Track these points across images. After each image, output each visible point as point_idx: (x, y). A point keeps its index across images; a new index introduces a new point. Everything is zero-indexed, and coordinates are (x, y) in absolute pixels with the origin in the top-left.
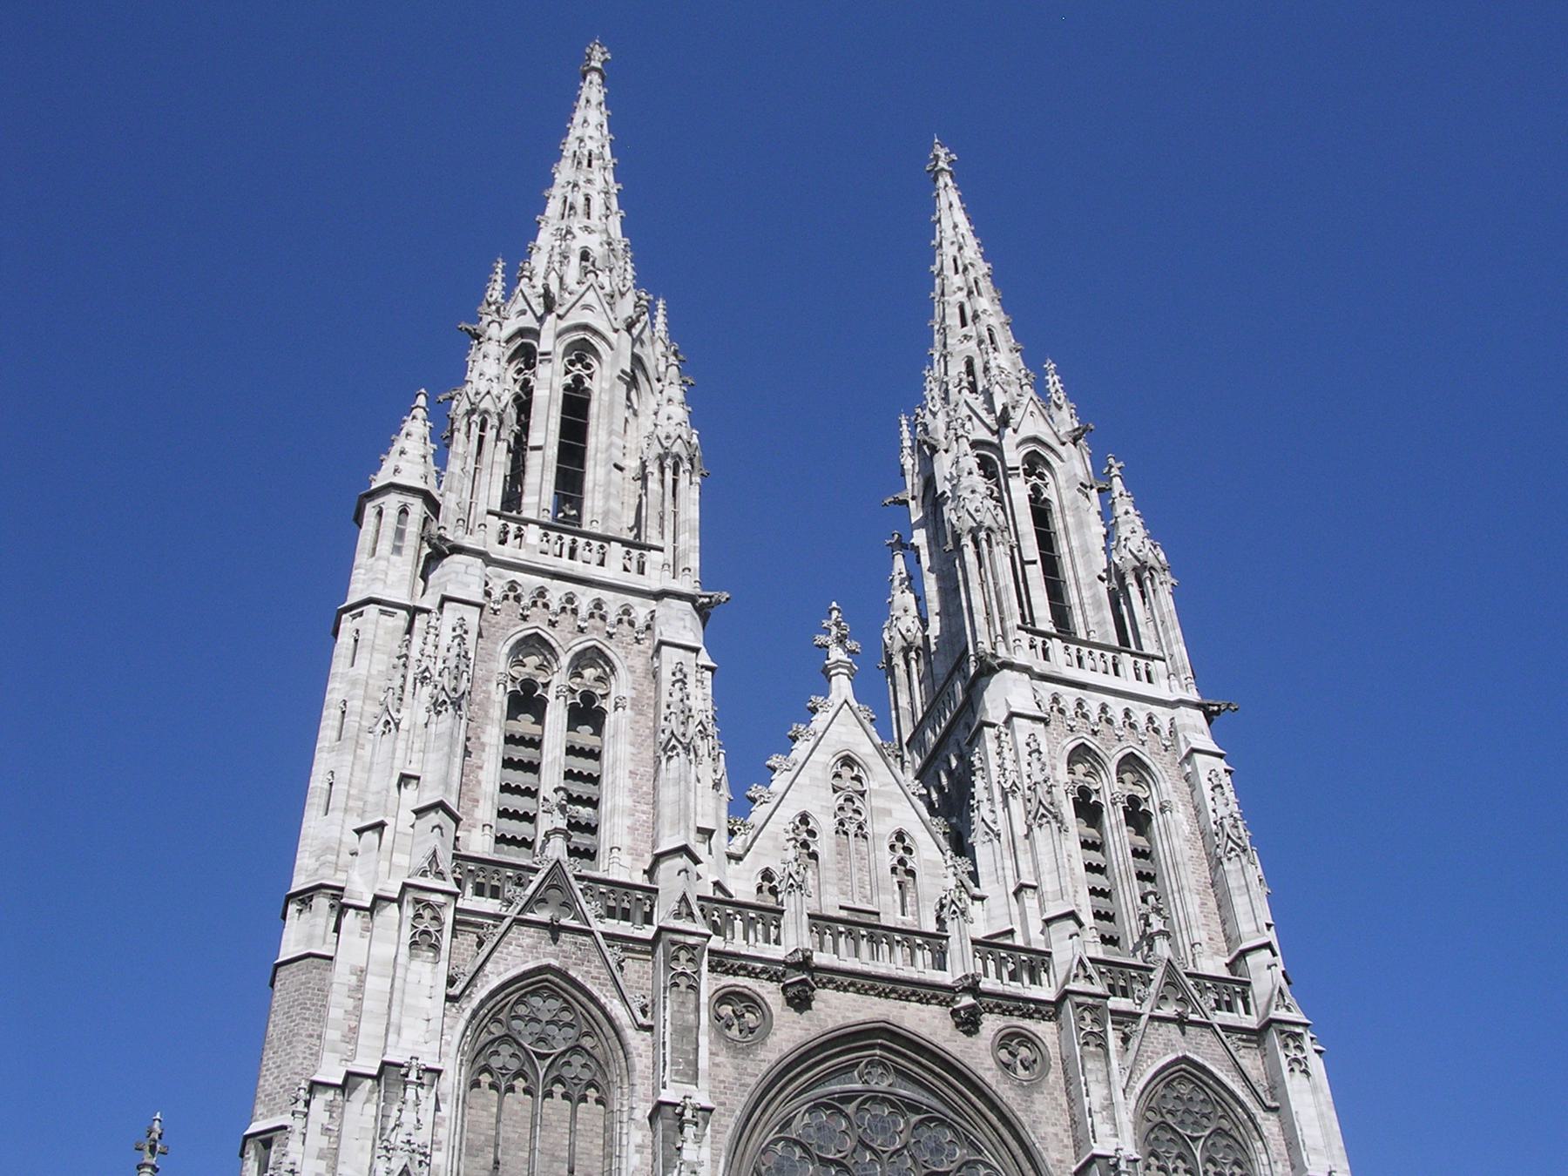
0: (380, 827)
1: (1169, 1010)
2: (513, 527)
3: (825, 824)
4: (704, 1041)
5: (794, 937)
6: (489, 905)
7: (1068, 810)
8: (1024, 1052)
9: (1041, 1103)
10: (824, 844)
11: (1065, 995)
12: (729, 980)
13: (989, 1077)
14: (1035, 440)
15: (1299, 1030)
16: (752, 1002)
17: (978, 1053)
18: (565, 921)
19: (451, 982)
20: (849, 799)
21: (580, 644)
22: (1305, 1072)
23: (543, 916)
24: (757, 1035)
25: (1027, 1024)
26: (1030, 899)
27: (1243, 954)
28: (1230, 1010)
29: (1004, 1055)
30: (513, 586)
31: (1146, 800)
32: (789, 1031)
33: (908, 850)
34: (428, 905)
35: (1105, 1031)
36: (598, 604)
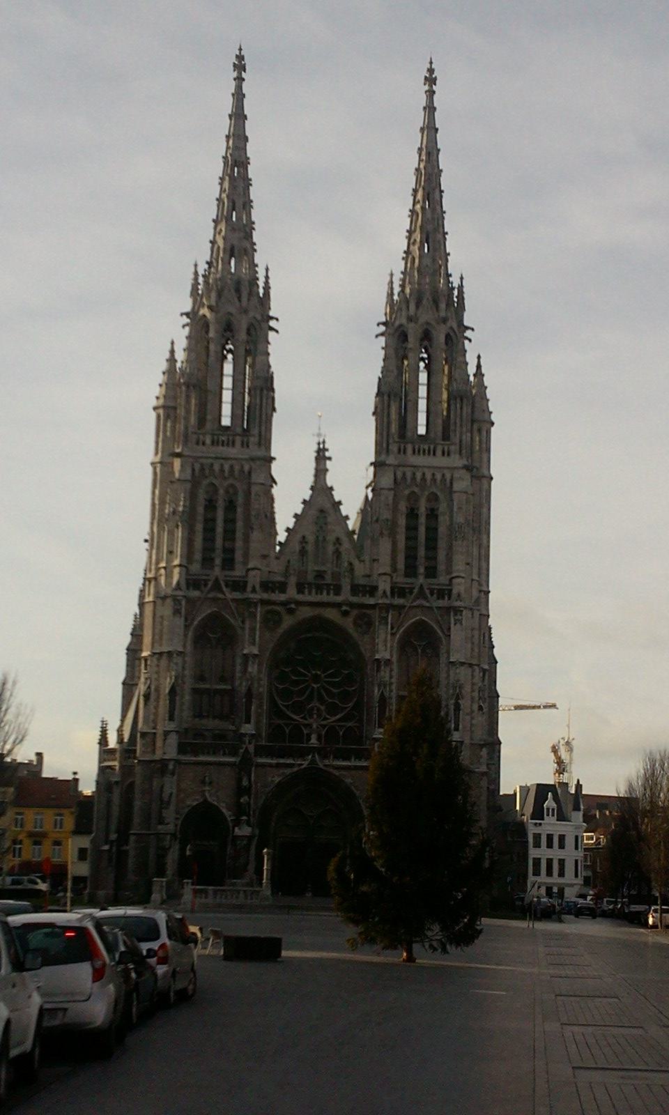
0: (165, 568)
1: (417, 603)
2: (201, 437)
3: (311, 539)
4: (258, 633)
5: (292, 592)
6: (196, 593)
7: (402, 521)
8: (366, 619)
9: (366, 638)
10: (310, 548)
11: (377, 604)
12: (270, 607)
13: (351, 631)
14: (428, 323)
15: (462, 609)
16: (278, 613)
17: (348, 624)
18: (221, 596)
19: (186, 620)
20: (321, 527)
21: (226, 484)
22: (461, 624)
23: (210, 595)
24: (279, 622)
25: (368, 612)
26: (375, 564)
27: (453, 578)
28: (443, 598)
29: (360, 622)
30: (202, 465)
31: (438, 509)
32: (288, 622)
33: (340, 544)
34: (178, 600)
35: (388, 616)
36: (232, 467)
